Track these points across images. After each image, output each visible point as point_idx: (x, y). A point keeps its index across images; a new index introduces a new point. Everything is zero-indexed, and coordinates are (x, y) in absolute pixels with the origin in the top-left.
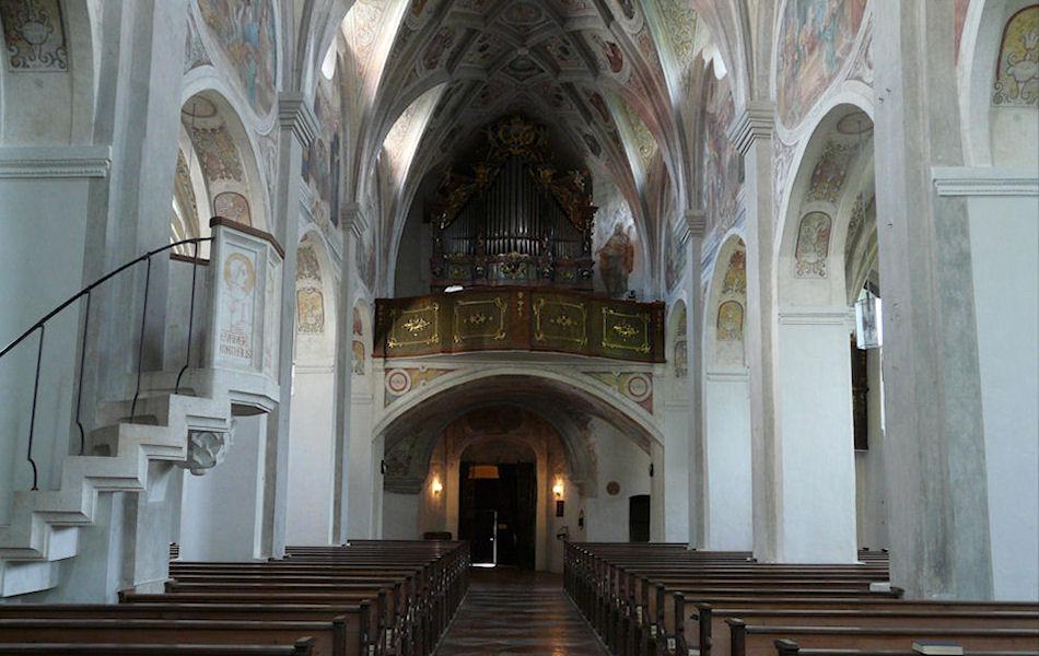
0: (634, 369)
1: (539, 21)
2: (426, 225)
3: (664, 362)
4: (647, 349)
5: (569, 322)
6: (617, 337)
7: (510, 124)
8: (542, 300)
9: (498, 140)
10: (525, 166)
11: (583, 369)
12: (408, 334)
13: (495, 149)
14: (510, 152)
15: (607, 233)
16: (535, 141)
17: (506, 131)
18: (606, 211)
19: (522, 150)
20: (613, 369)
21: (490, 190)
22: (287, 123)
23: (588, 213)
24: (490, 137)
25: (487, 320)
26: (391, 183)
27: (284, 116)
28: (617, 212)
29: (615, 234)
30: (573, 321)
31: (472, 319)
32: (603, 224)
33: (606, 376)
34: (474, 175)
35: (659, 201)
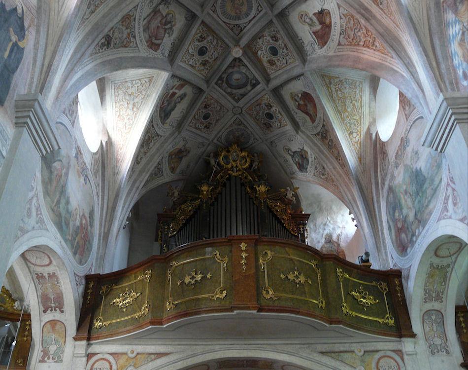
0: (380, 346)
1: (250, 17)
2: (157, 242)
3: (413, 335)
4: (391, 322)
5: (302, 279)
6: (356, 305)
7: (228, 151)
8: (269, 252)
9: (219, 164)
10: (242, 185)
11: (320, 348)
12: (119, 311)
13: (216, 173)
14: (229, 174)
15: (319, 242)
16: (251, 166)
17: (226, 157)
18: (315, 225)
19: (240, 173)
20: (354, 347)
21: (212, 204)
22: (21, 121)
23: (301, 219)
24: (212, 162)
25: (204, 278)
26: (115, 174)
27: (20, 115)
28: (325, 225)
29: (326, 243)
30: (307, 277)
31: (187, 280)
32: (313, 235)
33: (346, 355)
34: (199, 192)
35: (373, 181)
